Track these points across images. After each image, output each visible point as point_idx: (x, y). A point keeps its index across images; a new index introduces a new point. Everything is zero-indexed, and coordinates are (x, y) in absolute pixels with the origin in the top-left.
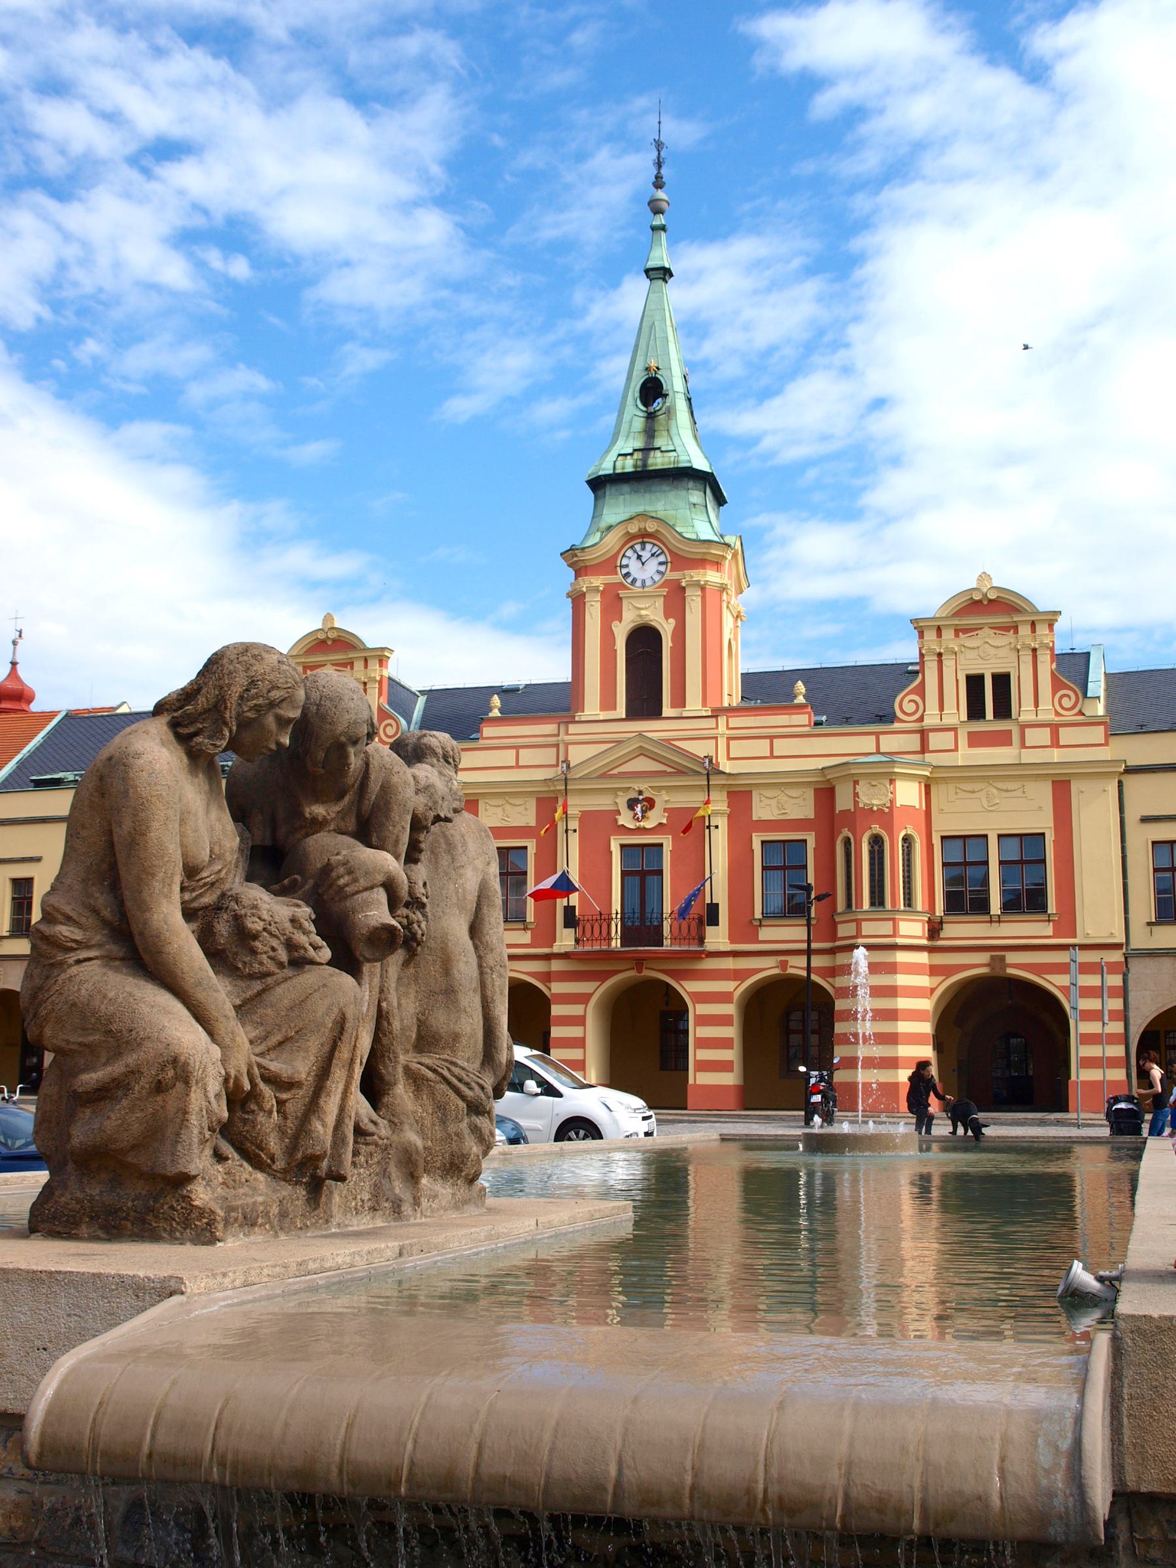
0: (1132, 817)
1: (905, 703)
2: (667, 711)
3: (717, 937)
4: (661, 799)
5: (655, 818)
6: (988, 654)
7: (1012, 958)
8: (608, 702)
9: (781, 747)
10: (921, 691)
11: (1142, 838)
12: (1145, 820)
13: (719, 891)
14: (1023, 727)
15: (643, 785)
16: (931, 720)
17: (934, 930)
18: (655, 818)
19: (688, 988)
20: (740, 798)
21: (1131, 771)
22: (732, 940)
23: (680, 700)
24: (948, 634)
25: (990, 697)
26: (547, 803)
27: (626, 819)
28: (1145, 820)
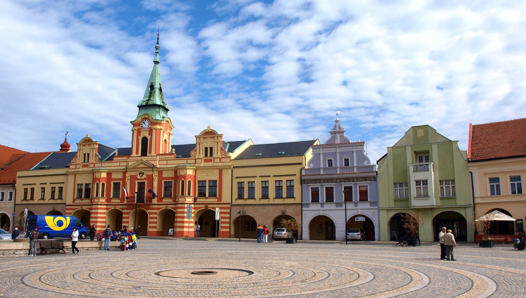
0: (234, 177)
1: (192, 153)
2: (148, 155)
3: (155, 201)
4: (146, 173)
5: (144, 176)
6: (209, 143)
7: (209, 206)
8: (137, 153)
9: (169, 162)
10: (196, 151)
11: (236, 181)
12: (236, 178)
13: (155, 191)
14: (214, 158)
15: (142, 170)
16: (197, 157)
17: (195, 200)
18: (144, 176)
19: (148, 211)
20: (160, 172)
21: (234, 167)
22: (158, 201)
23: (150, 153)
24: (202, 139)
25: (209, 152)
26: (124, 174)
27: (138, 177)
28: (236, 178)
